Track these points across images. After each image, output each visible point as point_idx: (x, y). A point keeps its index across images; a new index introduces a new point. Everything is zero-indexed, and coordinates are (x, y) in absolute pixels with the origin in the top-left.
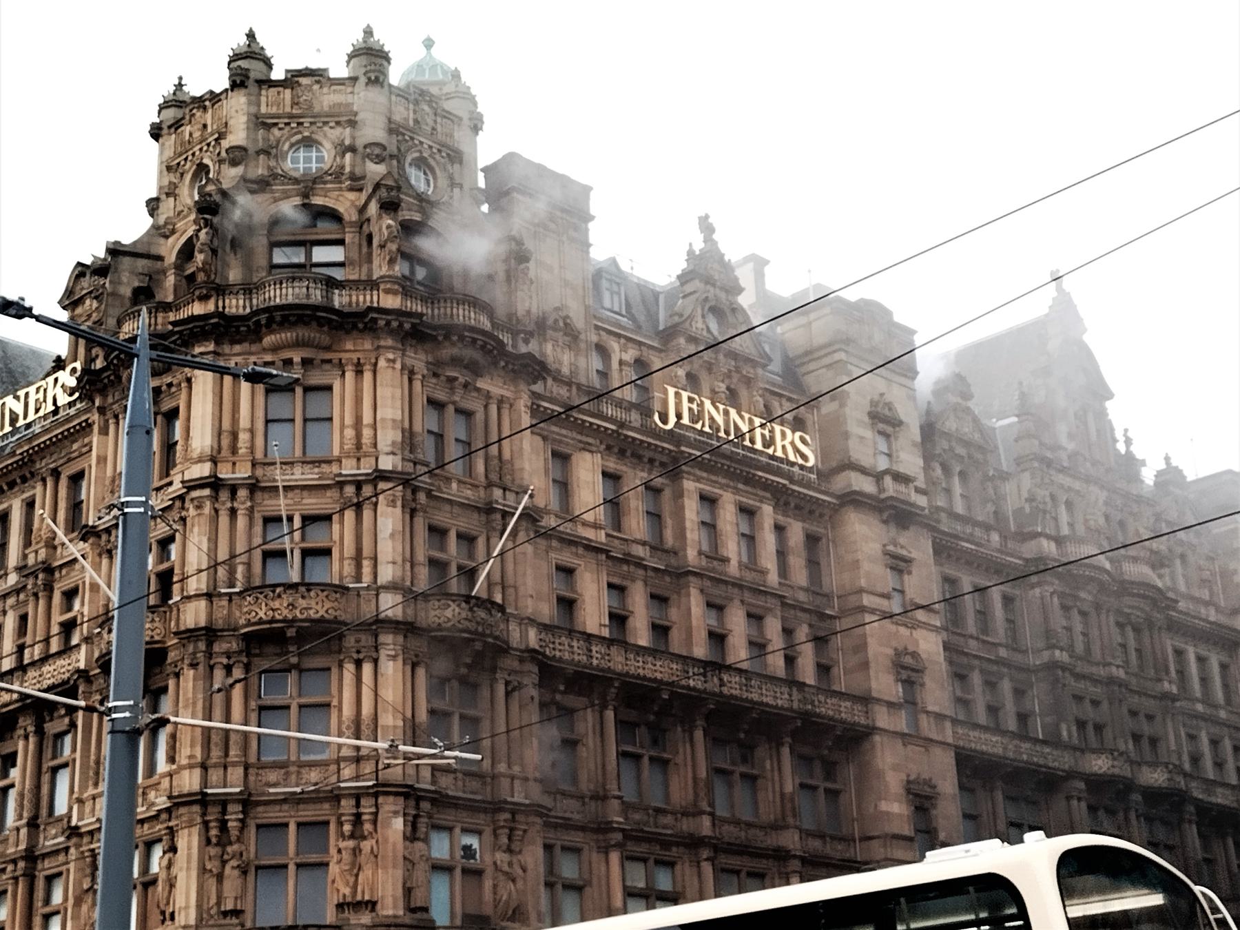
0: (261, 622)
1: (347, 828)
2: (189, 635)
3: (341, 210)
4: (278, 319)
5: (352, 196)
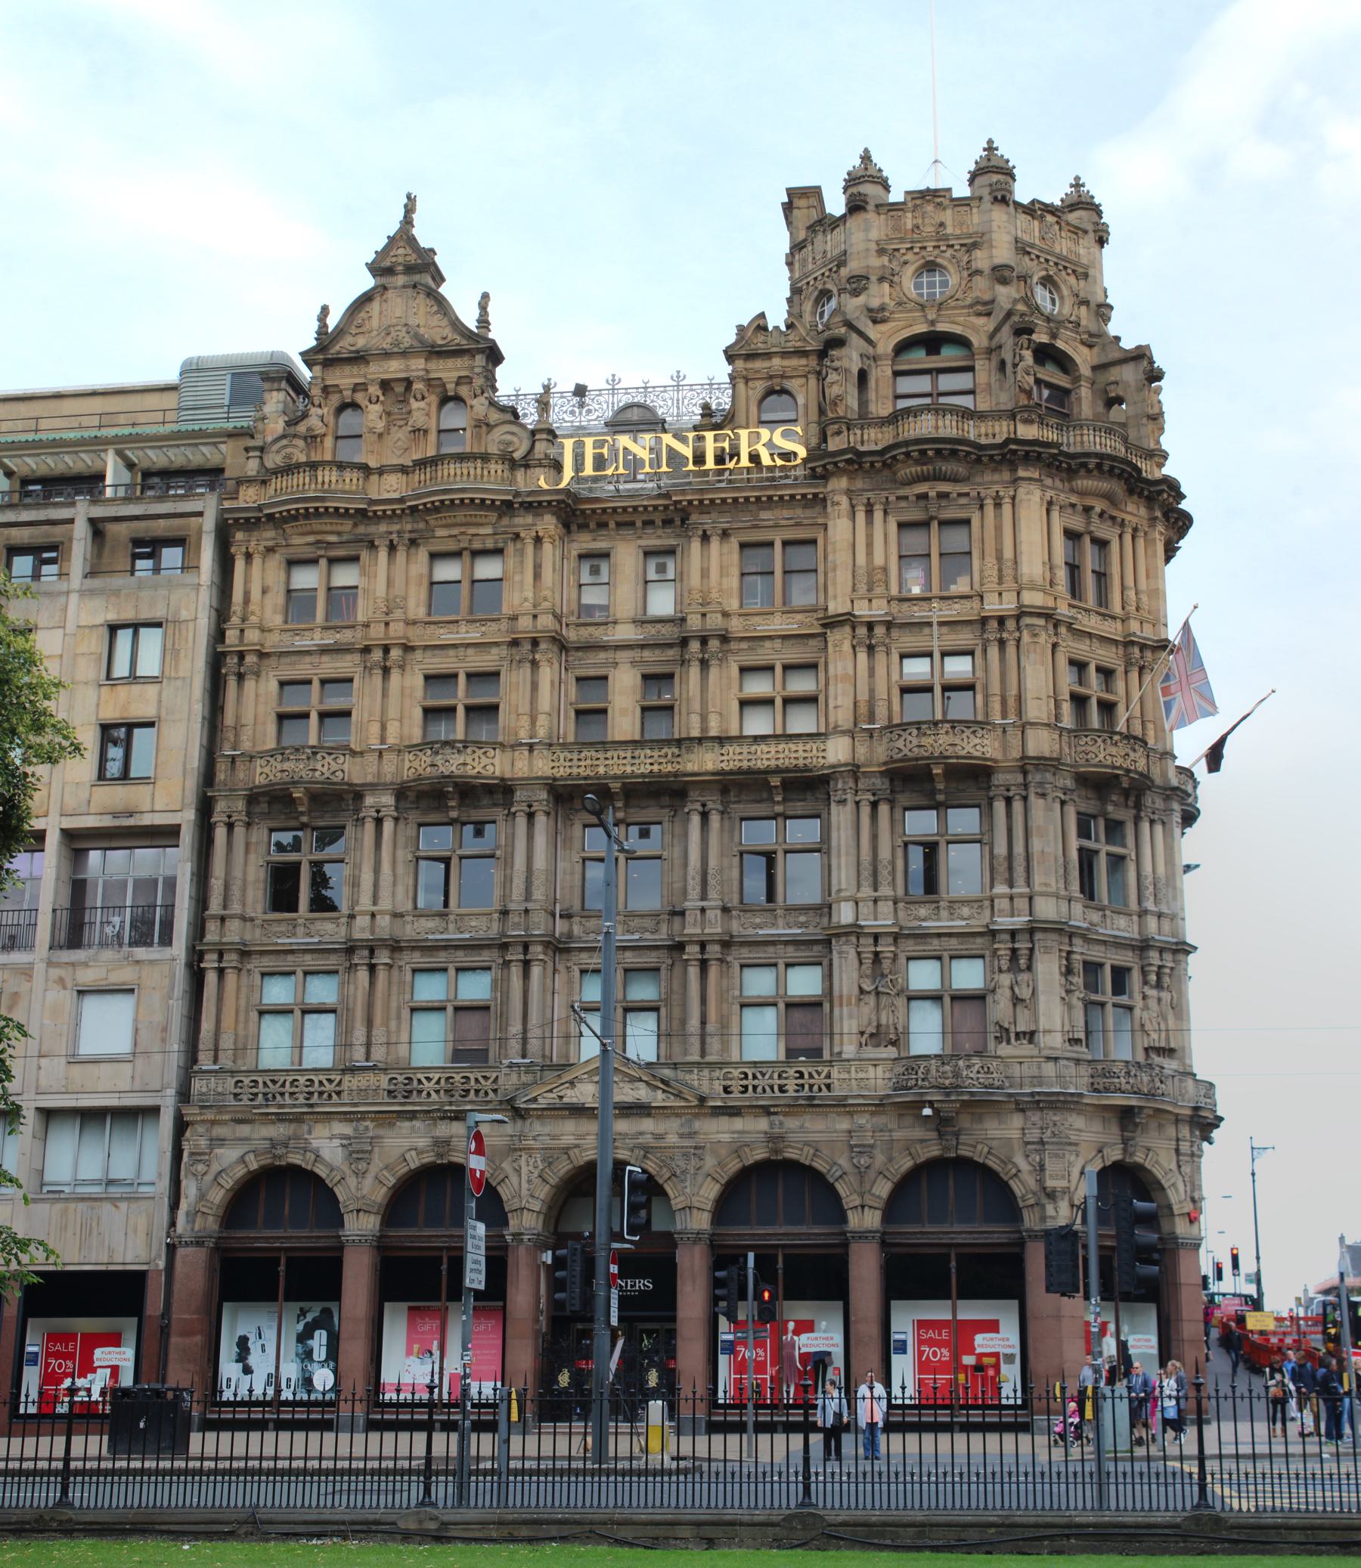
0: (1100, 765)
1: (1153, 978)
2: (1027, 765)
3: (1078, 360)
4: (1106, 468)
5: (1085, 350)
